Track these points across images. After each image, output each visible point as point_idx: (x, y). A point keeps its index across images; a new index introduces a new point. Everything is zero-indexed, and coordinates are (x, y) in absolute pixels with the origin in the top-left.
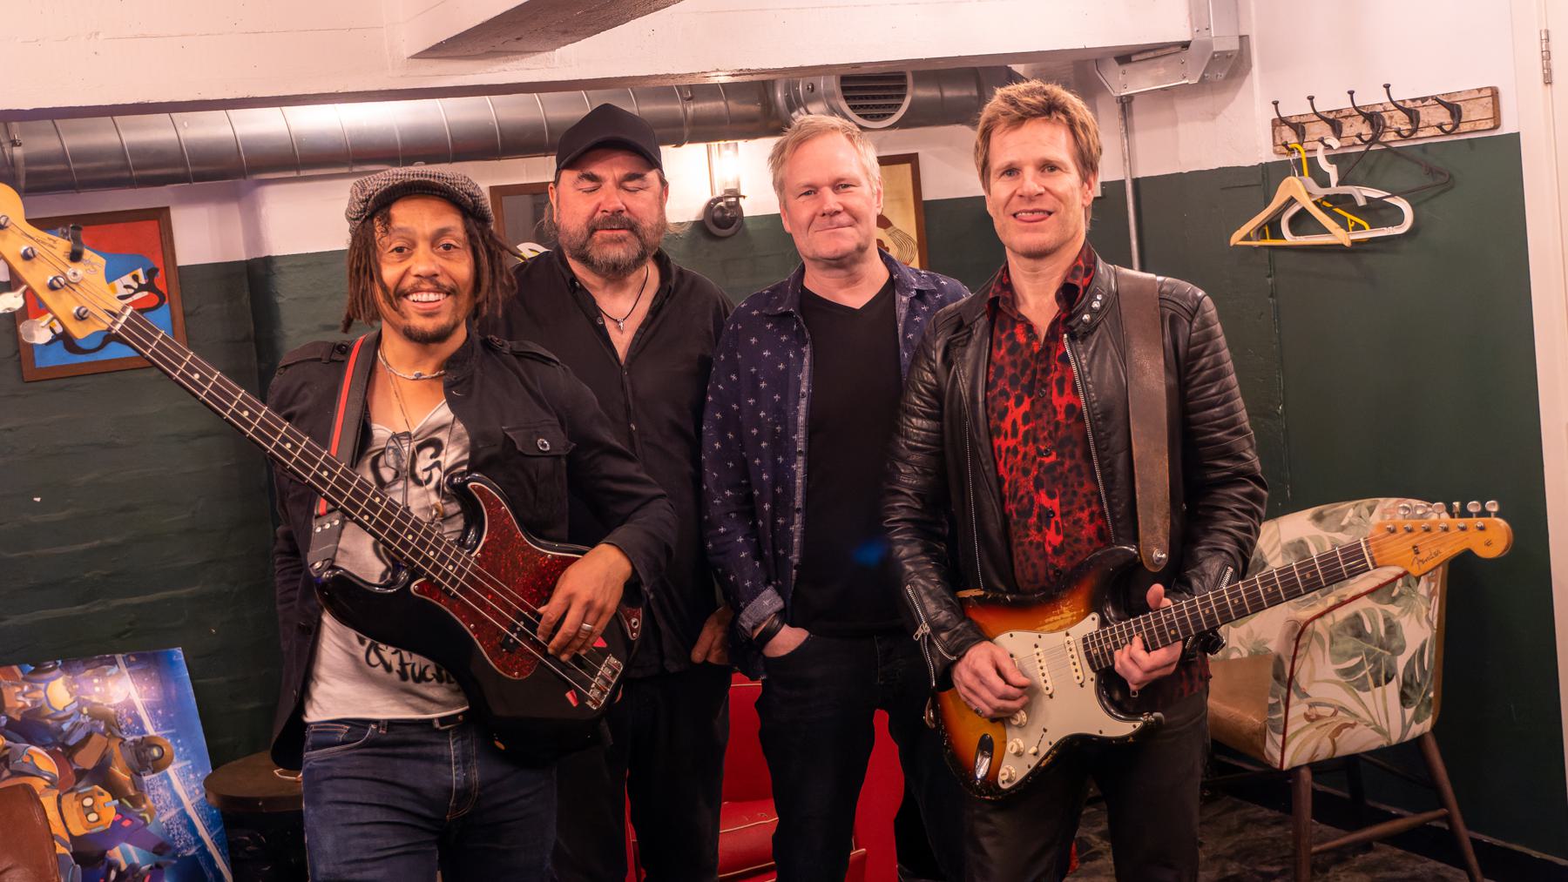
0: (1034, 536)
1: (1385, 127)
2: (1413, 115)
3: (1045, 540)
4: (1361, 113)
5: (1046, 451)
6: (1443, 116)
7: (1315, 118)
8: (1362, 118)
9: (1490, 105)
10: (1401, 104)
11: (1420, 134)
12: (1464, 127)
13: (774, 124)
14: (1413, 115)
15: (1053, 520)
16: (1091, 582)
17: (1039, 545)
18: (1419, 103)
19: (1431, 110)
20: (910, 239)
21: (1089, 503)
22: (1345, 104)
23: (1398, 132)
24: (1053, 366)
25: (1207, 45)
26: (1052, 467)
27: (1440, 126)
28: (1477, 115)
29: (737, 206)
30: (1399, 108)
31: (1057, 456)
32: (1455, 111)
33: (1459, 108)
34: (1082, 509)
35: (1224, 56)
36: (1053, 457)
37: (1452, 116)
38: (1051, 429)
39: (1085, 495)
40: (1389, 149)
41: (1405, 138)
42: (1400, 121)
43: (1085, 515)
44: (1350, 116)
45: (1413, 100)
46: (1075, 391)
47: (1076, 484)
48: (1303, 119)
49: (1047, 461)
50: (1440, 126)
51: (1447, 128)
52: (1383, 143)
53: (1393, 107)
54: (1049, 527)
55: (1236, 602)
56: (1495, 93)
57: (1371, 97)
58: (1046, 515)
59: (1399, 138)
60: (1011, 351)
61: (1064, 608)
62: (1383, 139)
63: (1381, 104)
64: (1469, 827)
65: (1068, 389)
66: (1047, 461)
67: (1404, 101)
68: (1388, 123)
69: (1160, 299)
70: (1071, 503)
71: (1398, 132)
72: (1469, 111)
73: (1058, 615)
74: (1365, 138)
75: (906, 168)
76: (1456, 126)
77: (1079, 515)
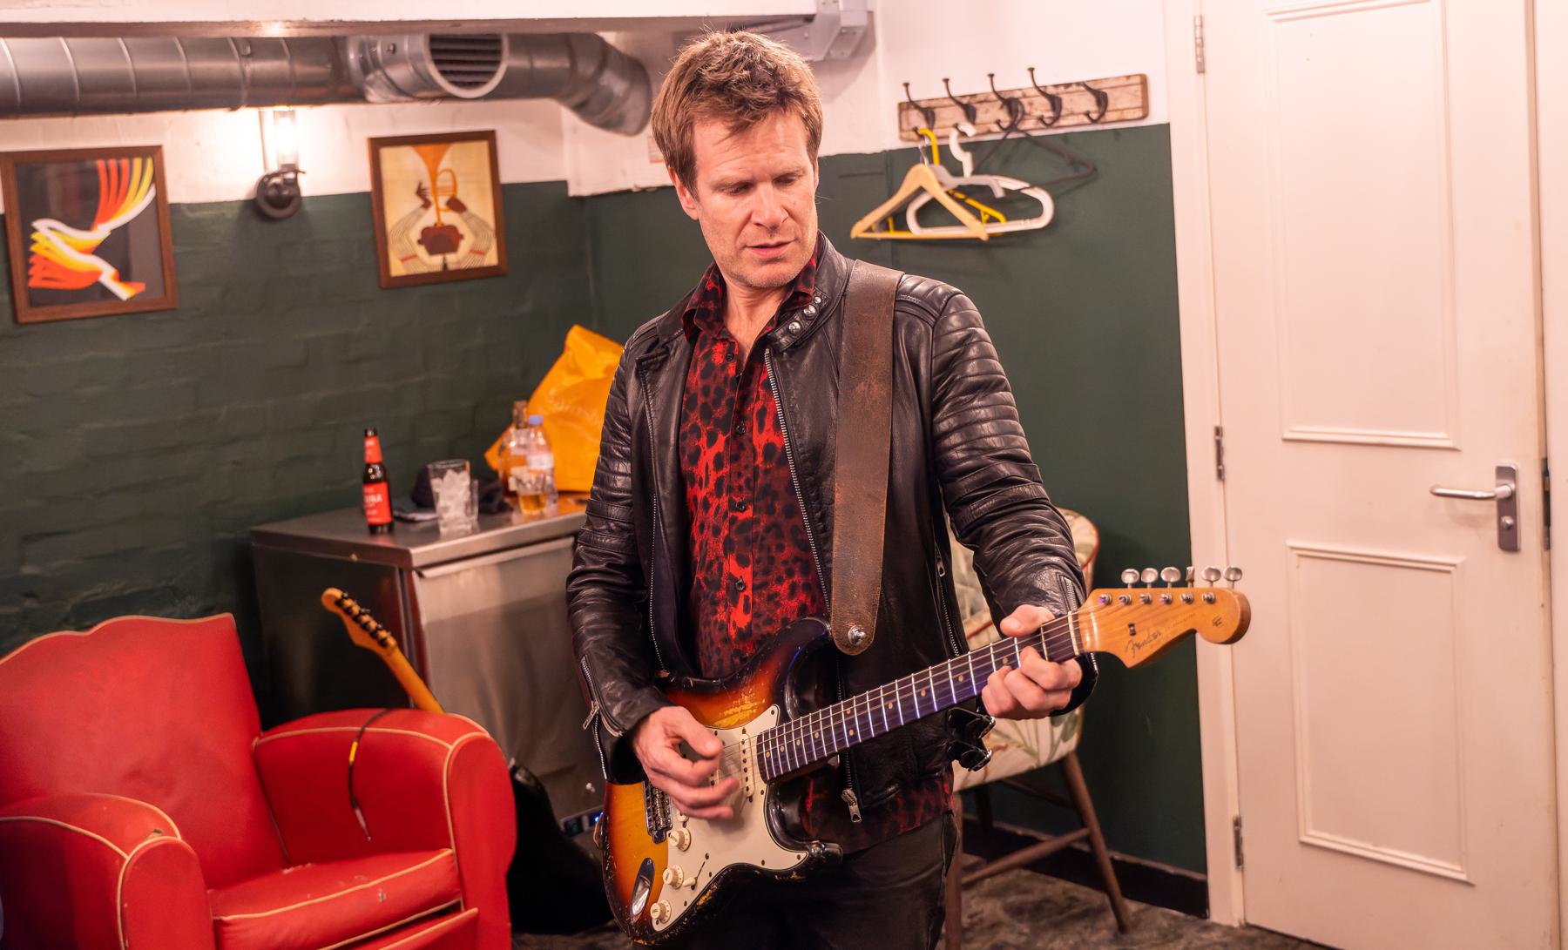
0: (721, 616)
1: (1024, 113)
2: (1055, 102)
3: (729, 620)
4: (1000, 98)
5: (740, 505)
6: (1088, 103)
7: (951, 102)
8: (1000, 103)
9: (1139, 94)
11: (1062, 122)
12: (1110, 116)
13: (343, 89)
14: (1055, 102)
15: (742, 595)
16: (777, 662)
17: (723, 627)
18: (1062, 89)
19: (1075, 97)
20: (487, 226)
21: (790, 573)
22: (983, 88)
24: (755, 395)
26: (747, 525)
27: (1087, 114)
28: (1123, 105)
29: (294, 184)
31: (755, 510)
32: (1101, 99)
33: (1105, 96)
34: (780, 580)
35: (845, 34)
36: (749, 513)
37: (1099, 103)
38: (749, 475)
39: (785, 562)
40: (1028, 137)
41: (1049, 126)
42: (1041, 107)
43: (783, 589)
44: (986, 101)
46: (777, 426)
47: (774, 547)
48: (933, 104)
49: (741, 517)
50: (1087, 114)
51: (1094, 116)
52: (1023, 131)
53: (1035, 92)
54: (735, 603)
55: (961, 679)
56: (1144, 81)
57: (1014, 81)
58: (735, 588)
59: (1041, 125)
60: (705, 375)
61: (746, 697)
62: (1022, 127)
63: (1020, 90)
64: (1111, 845)
65: (769, 422)
66: (741, 517)
67: (1045, 87)
68: (1027, 109)
69: (896, 301)
70: (767, 572)
72: (1116, 99)
73: (738, 706)
74: (1005, 125)
75: (483, 146)
76: (1102, 115)
77: (775, 588)
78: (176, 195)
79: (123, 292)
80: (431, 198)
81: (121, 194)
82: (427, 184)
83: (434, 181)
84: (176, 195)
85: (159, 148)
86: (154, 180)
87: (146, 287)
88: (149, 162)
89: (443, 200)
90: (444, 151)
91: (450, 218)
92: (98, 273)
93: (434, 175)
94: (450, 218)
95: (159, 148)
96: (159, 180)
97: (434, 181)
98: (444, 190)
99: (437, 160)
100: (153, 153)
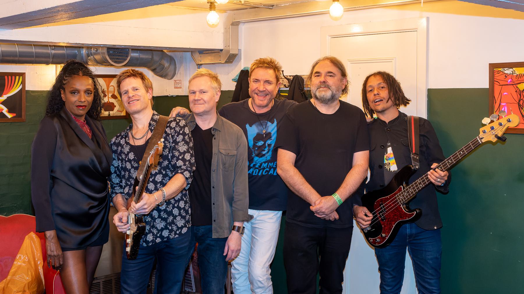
10: (286, 77)
23: (285, 86)
25: (229, 51)
30: (285, 78)
45: (290, 76)
53: (284, 78)
59: (285, 87)
67: (287, 76)
71: (285, 86)
78: (27, 88)
79: (9, 116)
80: (107, 94)
81: (11, 87)
82: (106, 90)
83: (108, 89)
84: (28, 88)
85: (24, 73)
86: (22, 83)
87: (16, 115)
88: (21, 77)
89: (110, 95)
90: (113, 80)
91: (112, 100)
92: (3, 110)
93: (108, 86)
94: (112, 100)
95: (24, 73)
96: (23, 83)
97: (108, 89)
98: (111, 92)
99: (110, 83)
100: (23, 75)
